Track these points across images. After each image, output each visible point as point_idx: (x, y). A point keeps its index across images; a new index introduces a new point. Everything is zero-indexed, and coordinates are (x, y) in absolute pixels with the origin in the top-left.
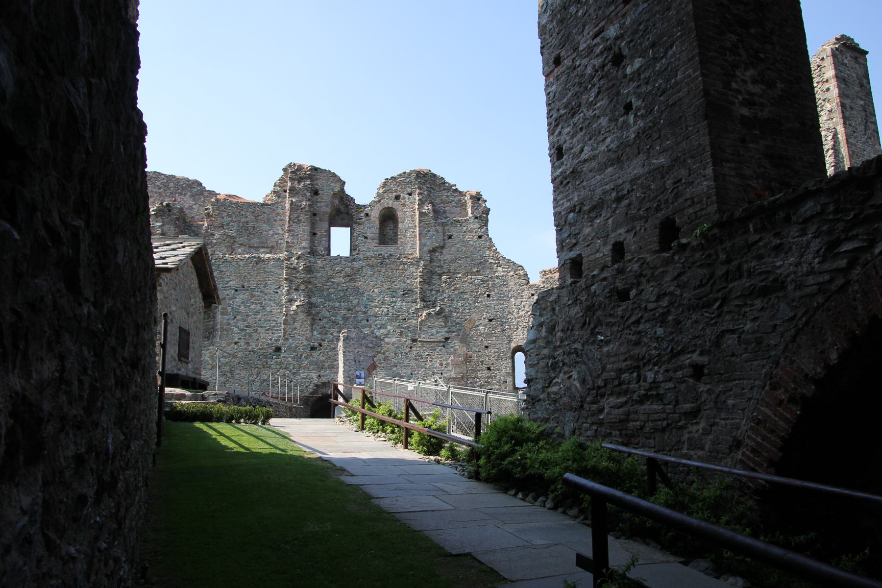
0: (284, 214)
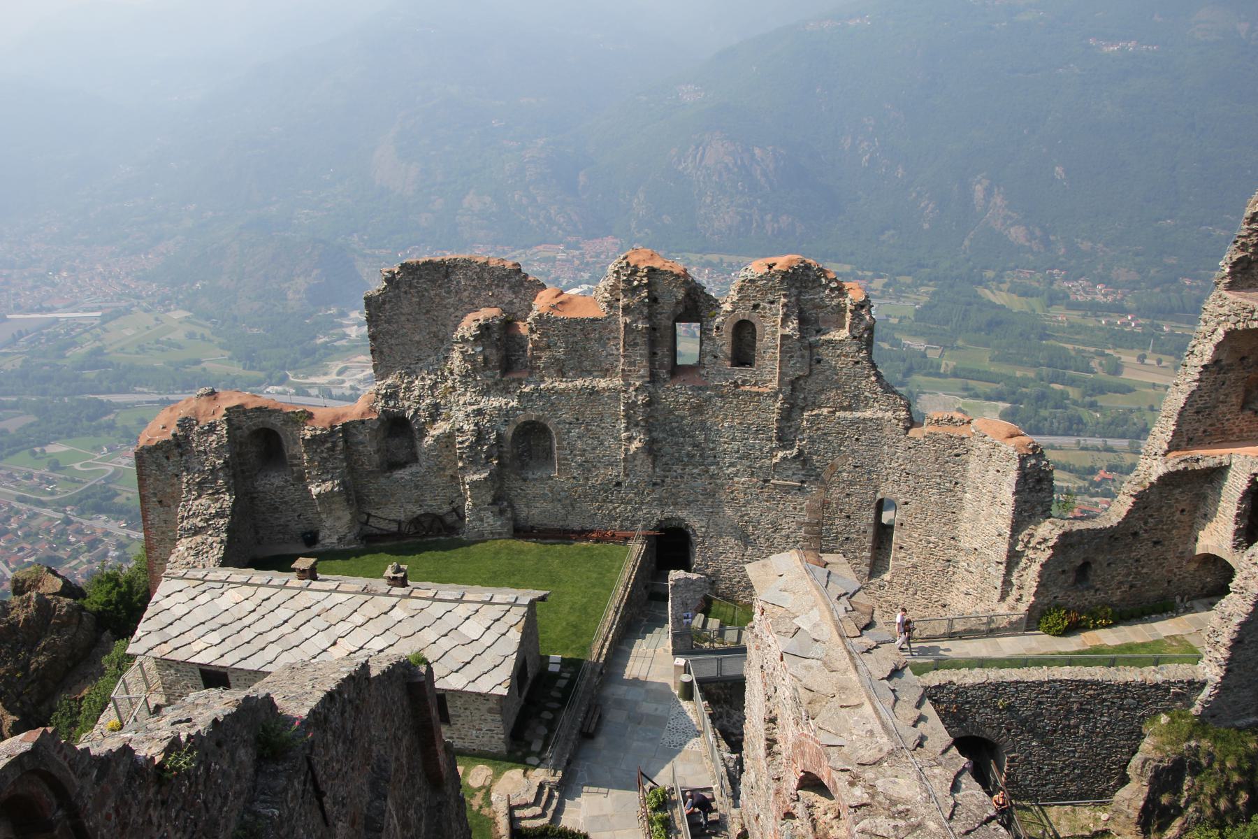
0: (618, 329)
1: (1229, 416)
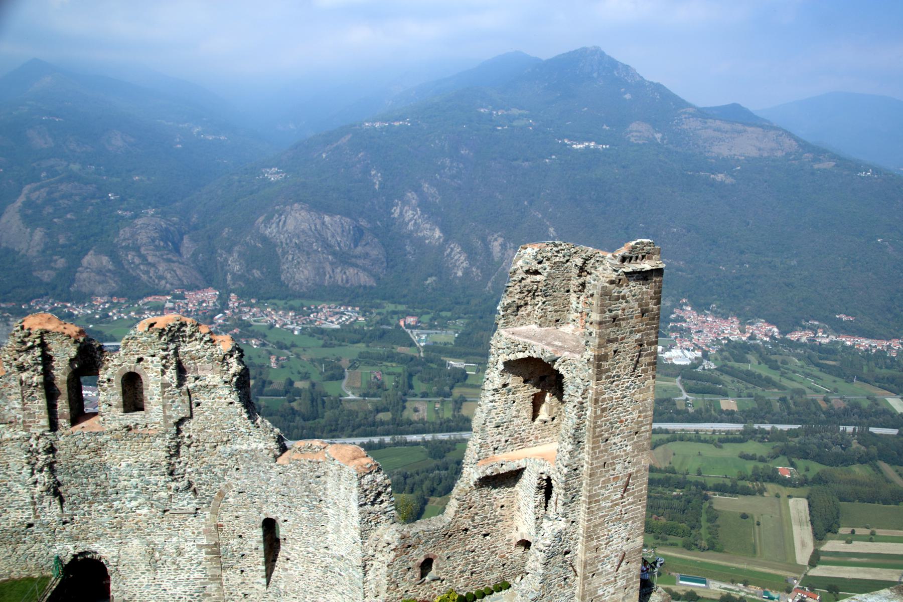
1: (523, 428)
